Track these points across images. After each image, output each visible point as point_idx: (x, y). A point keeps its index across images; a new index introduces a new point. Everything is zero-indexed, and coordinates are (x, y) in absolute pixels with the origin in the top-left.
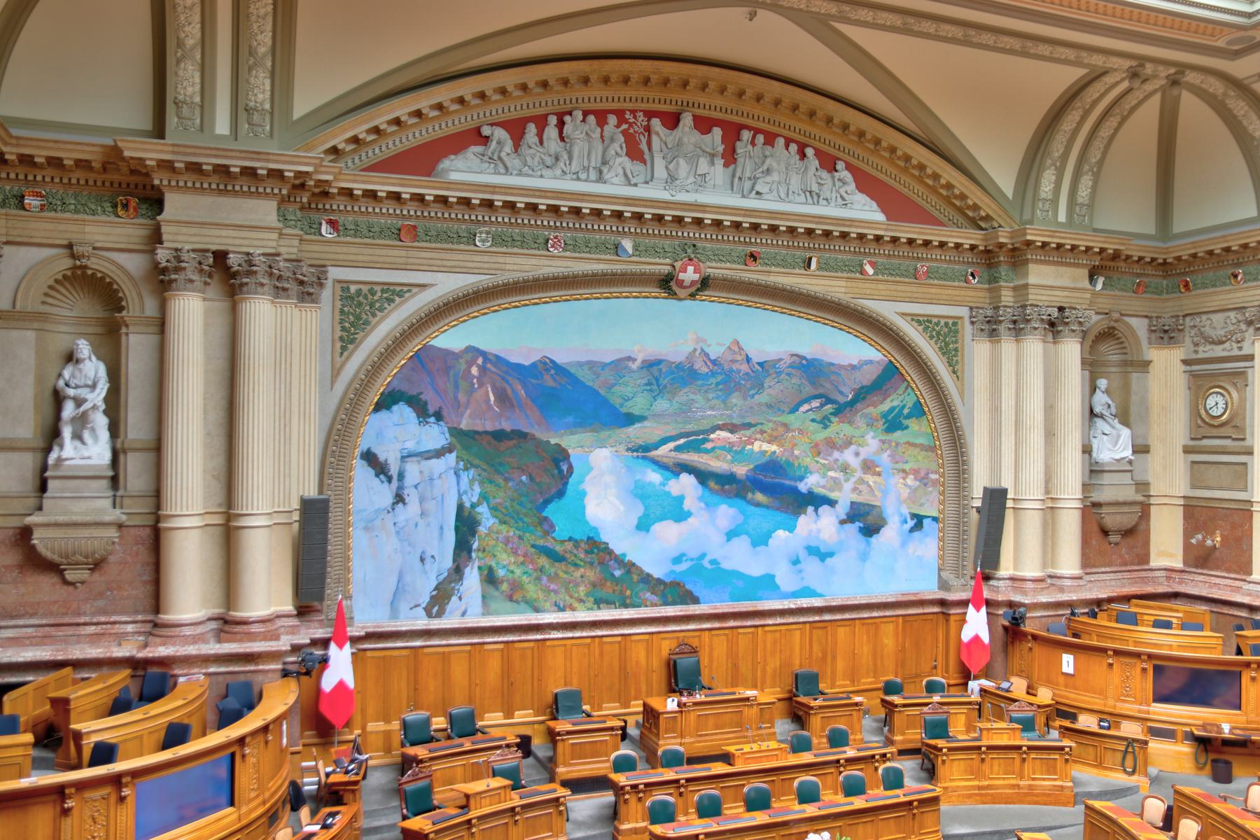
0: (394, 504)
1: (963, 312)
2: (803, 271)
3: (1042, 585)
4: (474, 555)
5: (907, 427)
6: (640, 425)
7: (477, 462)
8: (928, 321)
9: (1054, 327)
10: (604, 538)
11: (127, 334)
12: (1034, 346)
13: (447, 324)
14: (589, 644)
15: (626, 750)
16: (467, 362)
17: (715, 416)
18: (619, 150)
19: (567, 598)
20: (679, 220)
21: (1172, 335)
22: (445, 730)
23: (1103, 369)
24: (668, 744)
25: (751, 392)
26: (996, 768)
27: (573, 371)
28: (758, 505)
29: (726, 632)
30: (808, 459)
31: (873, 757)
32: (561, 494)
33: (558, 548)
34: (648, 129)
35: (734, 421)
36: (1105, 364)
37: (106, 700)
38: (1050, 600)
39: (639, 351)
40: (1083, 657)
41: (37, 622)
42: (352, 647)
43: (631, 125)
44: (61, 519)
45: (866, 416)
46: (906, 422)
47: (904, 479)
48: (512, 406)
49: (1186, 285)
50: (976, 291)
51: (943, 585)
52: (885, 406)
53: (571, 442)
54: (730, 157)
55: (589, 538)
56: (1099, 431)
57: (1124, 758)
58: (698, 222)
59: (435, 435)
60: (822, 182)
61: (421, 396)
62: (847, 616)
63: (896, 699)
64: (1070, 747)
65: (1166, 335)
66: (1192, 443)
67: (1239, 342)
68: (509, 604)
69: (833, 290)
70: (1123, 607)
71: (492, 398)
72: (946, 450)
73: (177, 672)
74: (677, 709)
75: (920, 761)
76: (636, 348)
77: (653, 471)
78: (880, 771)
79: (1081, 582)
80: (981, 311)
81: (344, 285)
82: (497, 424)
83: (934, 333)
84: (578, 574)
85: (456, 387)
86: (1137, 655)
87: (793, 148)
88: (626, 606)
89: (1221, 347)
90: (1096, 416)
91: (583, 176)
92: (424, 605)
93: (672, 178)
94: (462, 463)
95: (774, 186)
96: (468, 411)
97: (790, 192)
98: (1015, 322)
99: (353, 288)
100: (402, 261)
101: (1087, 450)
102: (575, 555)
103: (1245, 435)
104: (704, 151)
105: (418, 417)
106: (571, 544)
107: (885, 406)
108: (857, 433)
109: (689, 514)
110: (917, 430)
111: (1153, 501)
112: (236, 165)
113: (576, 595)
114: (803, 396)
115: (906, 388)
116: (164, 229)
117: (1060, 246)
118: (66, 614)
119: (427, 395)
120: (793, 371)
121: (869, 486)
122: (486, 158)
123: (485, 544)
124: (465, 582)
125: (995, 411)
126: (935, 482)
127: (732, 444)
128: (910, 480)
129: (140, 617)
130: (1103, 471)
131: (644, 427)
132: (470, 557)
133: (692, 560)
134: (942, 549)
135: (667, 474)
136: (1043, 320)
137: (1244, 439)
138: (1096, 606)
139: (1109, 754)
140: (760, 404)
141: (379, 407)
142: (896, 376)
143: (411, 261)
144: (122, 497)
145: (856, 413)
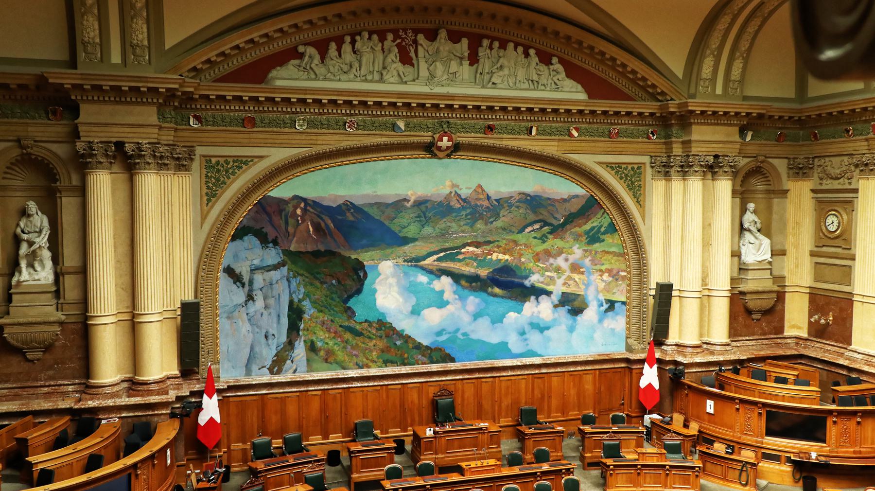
0: (246, 301)
1: (646, 159)
2: (526, 137)
3: (699, 350)
4: (301, 333)
5: (603, 241)
6: (413, 244)
7: (302, 272)
8: (619, 167)
9: (712, 169)
10: (389, 320)
11: (61, 198)
12: (695, 184)
13: (279, 182)
14: (379, 391)
15: (398, 462)
16: (294, 206)
17: (465, 236)
18: (394, 59)
19: (365, 360)
20: (436, 106)
21: (805, 171)
22: (281, 448)
23: (752, 196)
24: (427, 459)
25: (492, 220)
26: (648, 479)
27: (366, 209)
28: (495, 295)
29: (473, 381)
30: (532, 264)
31: (561, 470)
32: (359, 291)
33: (358, 327)
34: (415, 42)
35: (479, 240)
36: (754, 192)
37: (51, 437)
38: (703, 361)
39: (412, 195)
41: (10, 386)
42: (218, 396)
43: (403, 39)
44: (21, 320)
45: (572, 234)
46: (602, 237)
47: (601, 276)
48: (325, 234)
49: (815, 136)
50: (656, 144)
51: (629, 349)
52: (587, 227)
53: (366, 257)
54: (474, 59)
55: (379, 320)
56: (747, 241)
57: (740, 475)
58: (450, 107)
59: (272, 256)
60: (541, 73)
61: (263, 230)
62: (559, 370)
63: (587, 429)
64: (699, 467)
65: (800, 171)
66: (816, 249)
67: (849, 179)
68: (325, 364)
69: (548, 148)
70: (759, 366)
71: (311, 230)
72: (632, 256)
73: (101, 416)
74: (433, 435)
75: (600, 471)
76: (409, 193)
77: (422, 275)
78: (563, 481)
79: (728, 348)
80: (659, 159)
81: (207, 158)
82: (315, 247)
83: (623, 175)
84: (371, 344)
85: (287, 223)
86: (755, 403)
87: (520, 49)
88: (404, 364)
89: (837, 182)
90: (746, 230)
91: (369, 77)
92: (268, 367)
93: (432, 76)
94: (292, 273)
95: (506, 78)
96: (295, 239)
97: (518, 81)
98: (682, 166)
99: (214, 160)
100: (246, 141)
101: (736, 254)
102: (370, 332)
103: (851, 246)
104: (455, 56)
105: (262, 244)
106: (366, 324)
107: (587, 227)
108: (567, 245)
109: (448, 303)
110: (611, 243)
111: (787, 289)
112: (125, 86)
113: (370, 358)
114: (528, 221)
115: (603, 214)
116: (80, 128)
117: (715, 113)
118: (29, 380)
119: (269, 230)
120: (521, 205)
121: (576, 282)
122: (302, 68)
123: (308, 326)
124: (295, 351)
125: (667, 228)
126: (624, 278)
127: (477, 255)
128: (606, 277)
129: (77, 381)
130: (748, 270)
131: (416, 246)
132: (299, 334)
133: (450, 333)
134: (628, 323)
135: (433, 277)
136: (701, 166)
137: (850, 249)
138: (738, 365)
139: (731, 471)
140: (497, 228)
141: (234, 238)
142: (596, 206)
143: (253, 140)
144: (62, 304)
145: (567, 231)
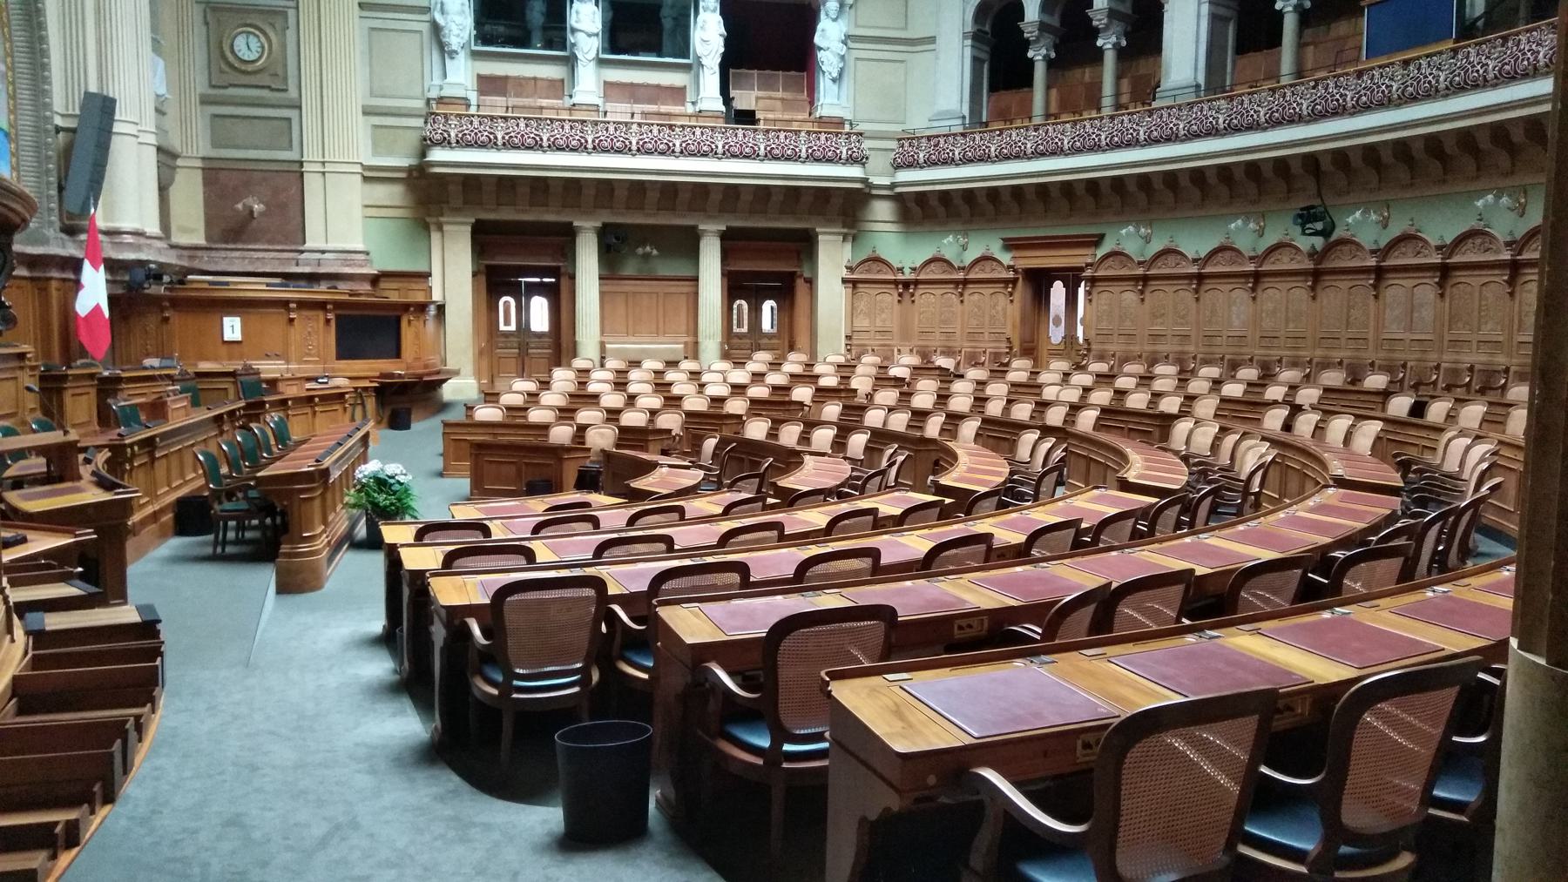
40: (255, 316)
103: (287, 84)
